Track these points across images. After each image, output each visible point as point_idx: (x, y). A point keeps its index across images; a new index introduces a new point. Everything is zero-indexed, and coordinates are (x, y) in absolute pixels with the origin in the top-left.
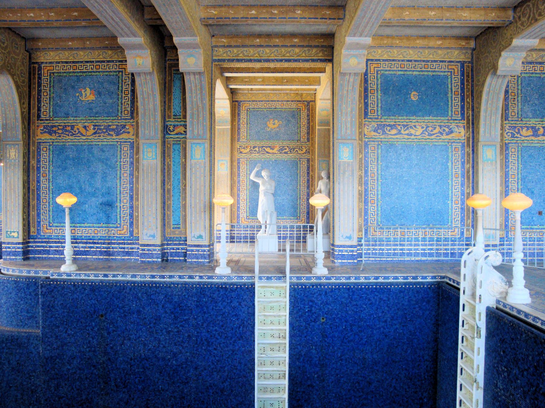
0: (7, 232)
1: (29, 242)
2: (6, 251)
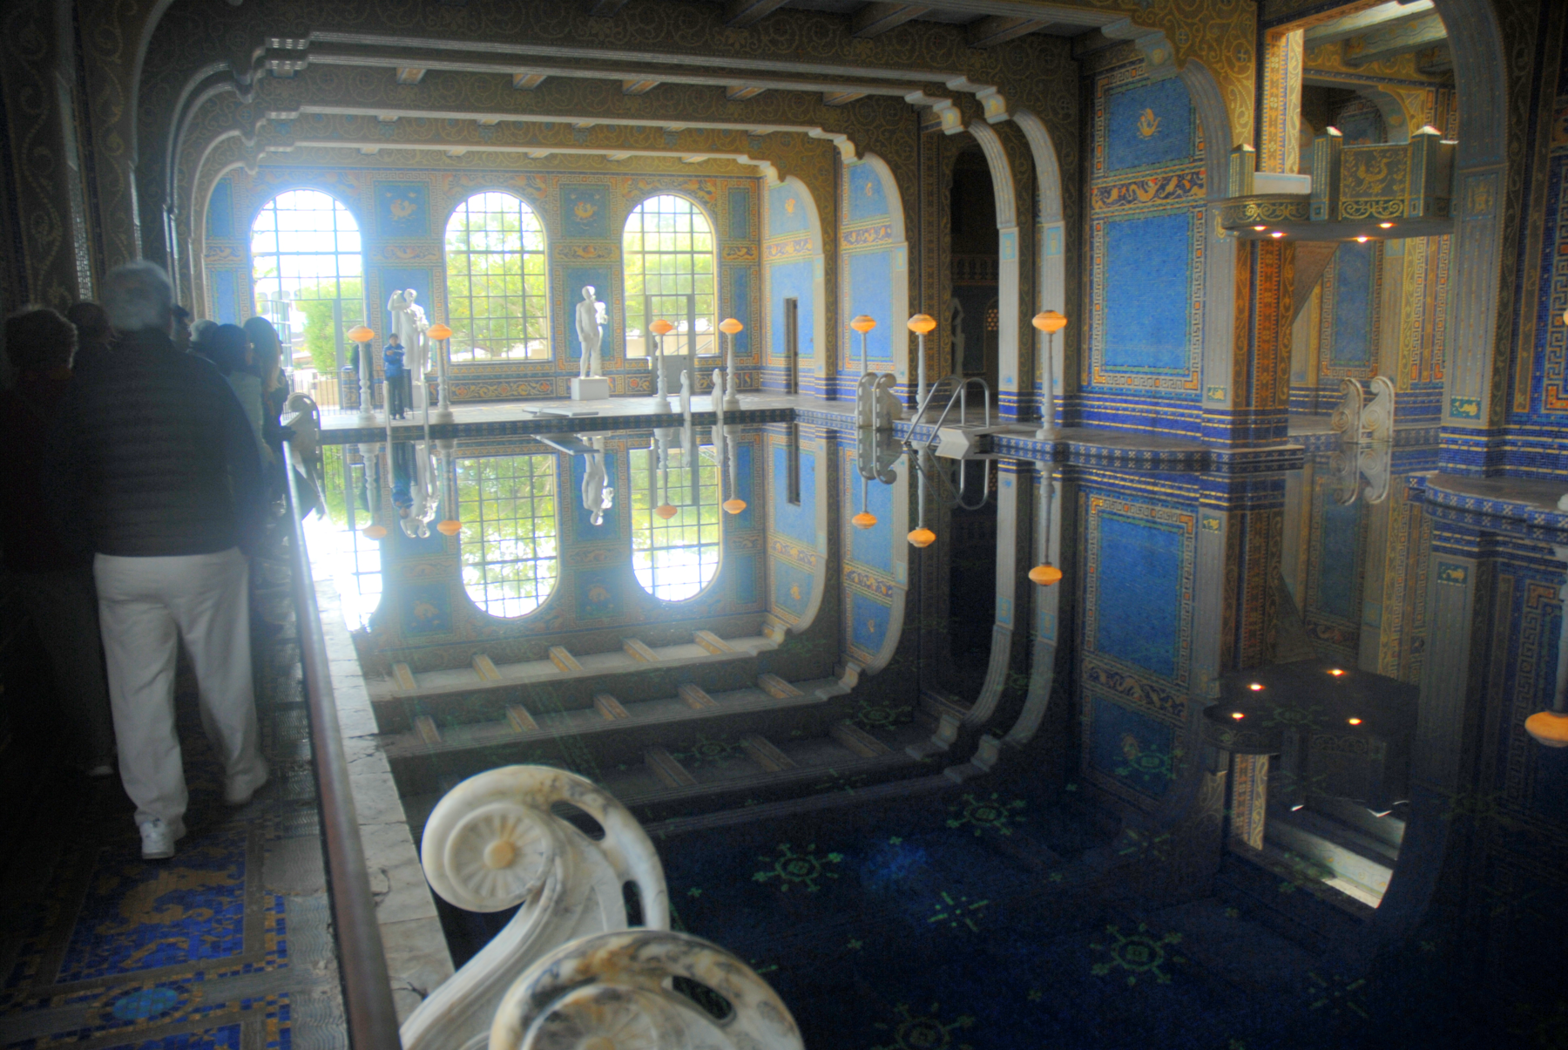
0: (1453, 401)
1: (1507, 432)
2: (1447, 450)
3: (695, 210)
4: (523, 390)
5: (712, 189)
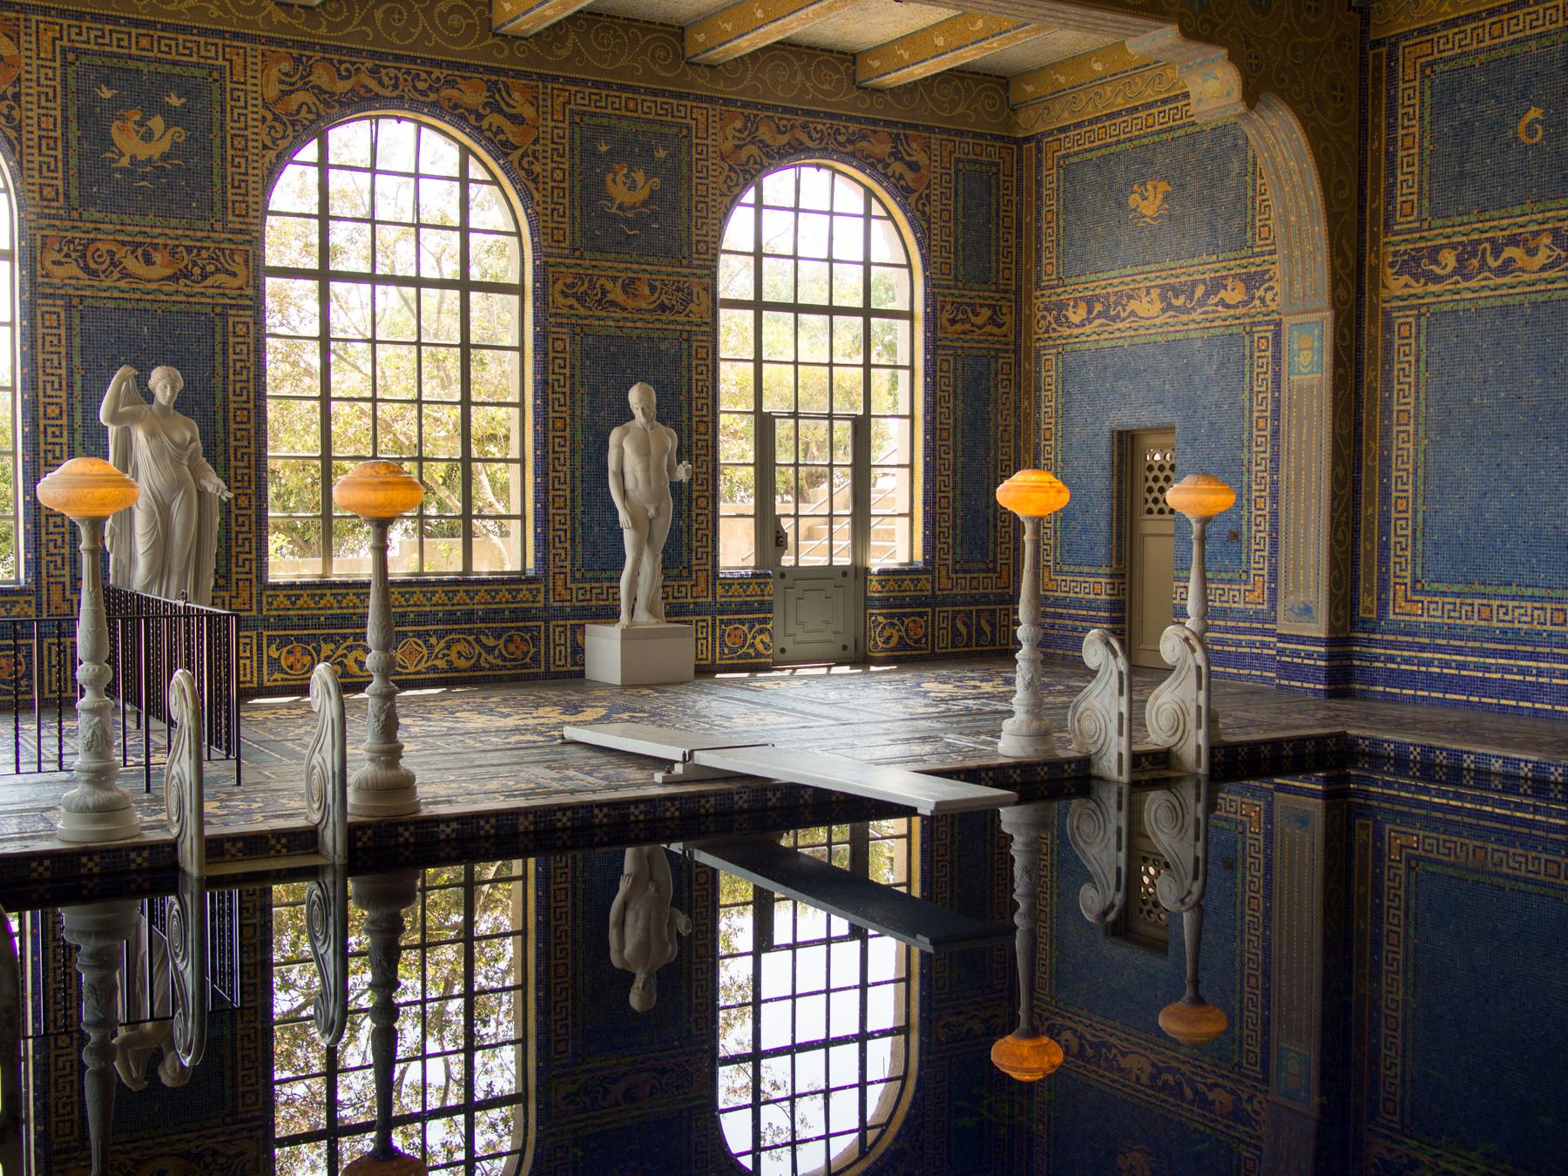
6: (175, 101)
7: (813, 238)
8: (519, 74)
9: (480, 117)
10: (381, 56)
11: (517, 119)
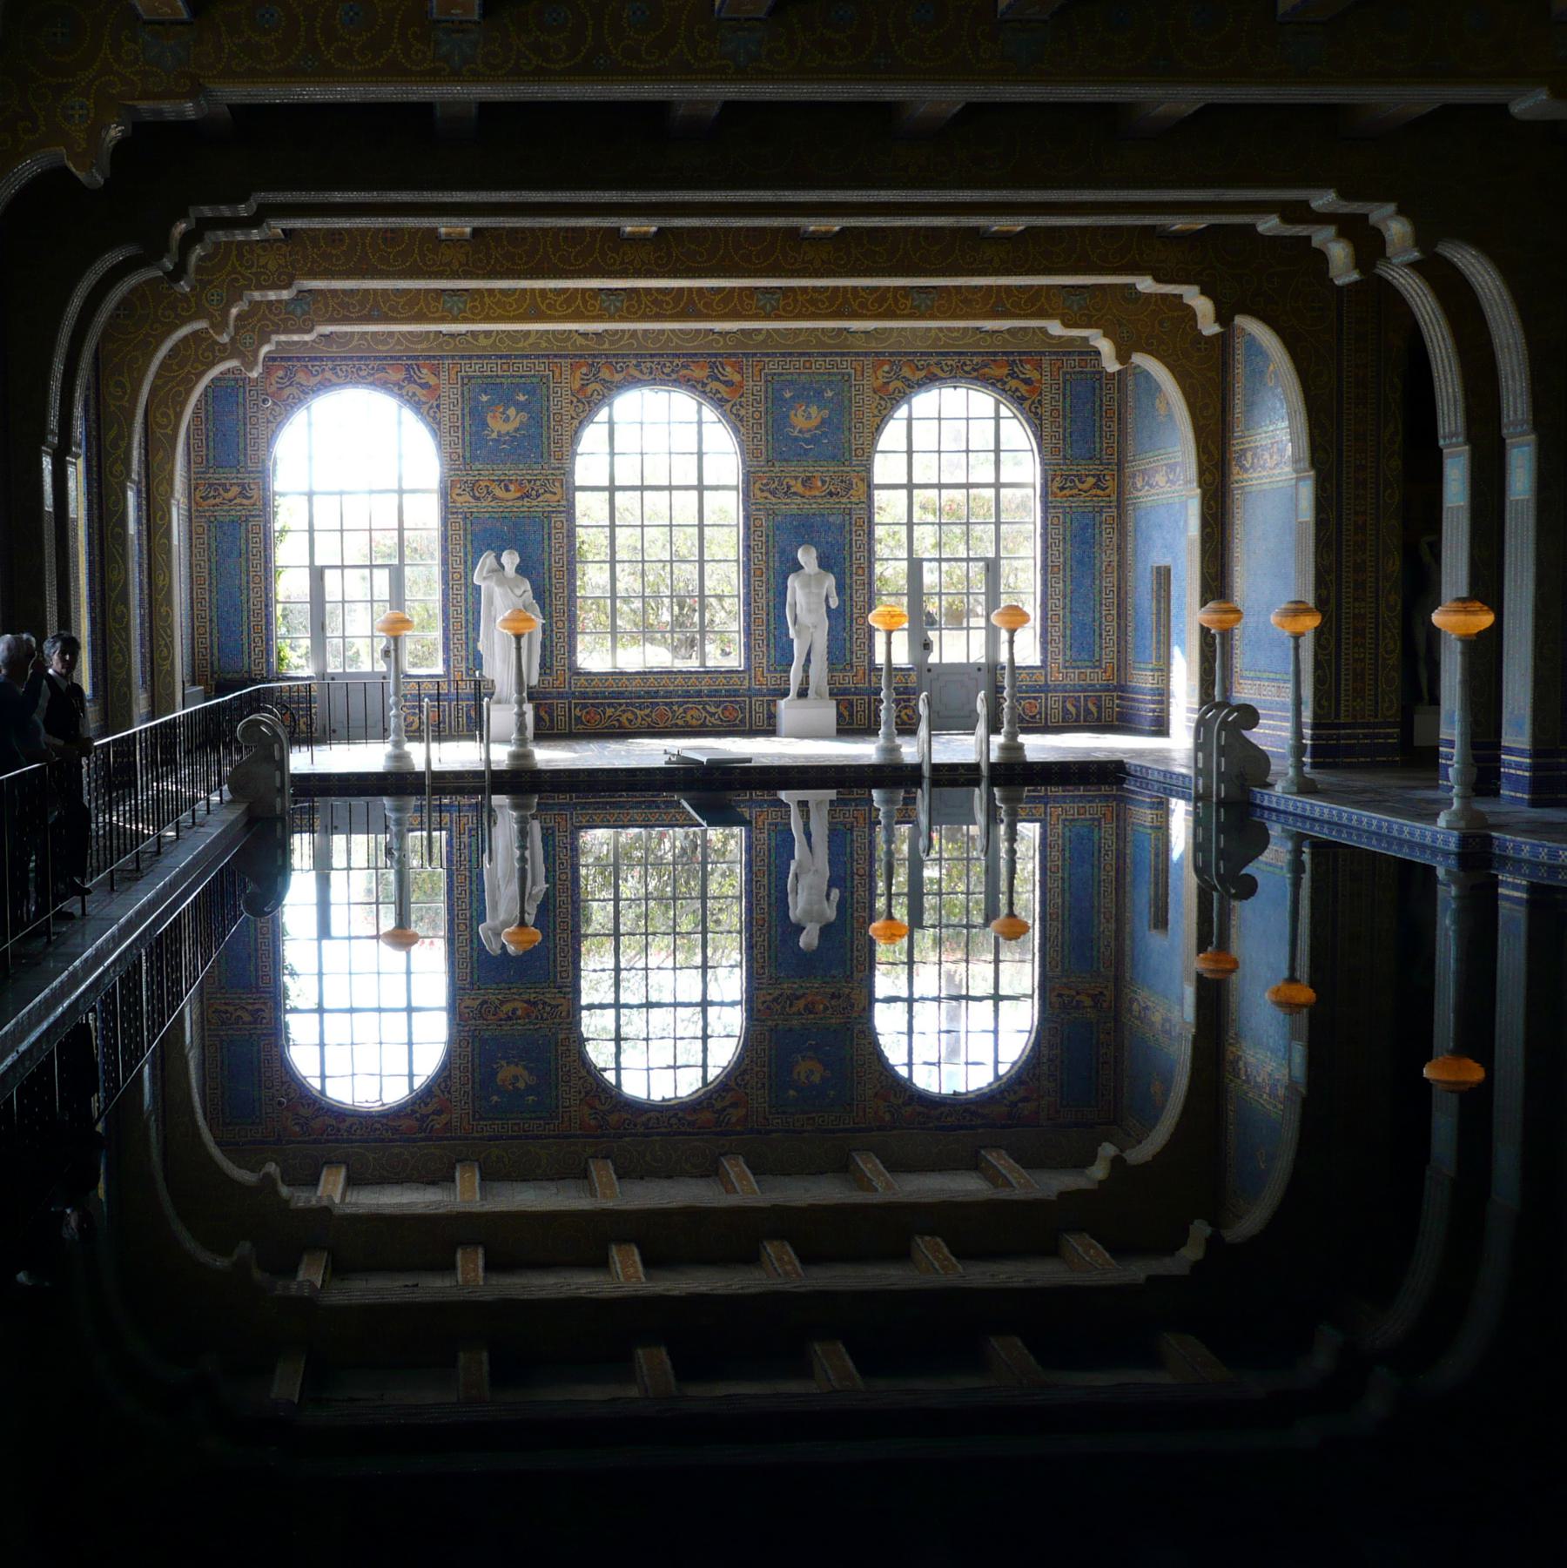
3: (1004, 411)
4: (694, 716)
5: (1035, 375)
6: (522, 398)
7: (952, 436)
8: (730, 355)
9: (704, 385)
10: (642, 356)
11: (728, 383)
